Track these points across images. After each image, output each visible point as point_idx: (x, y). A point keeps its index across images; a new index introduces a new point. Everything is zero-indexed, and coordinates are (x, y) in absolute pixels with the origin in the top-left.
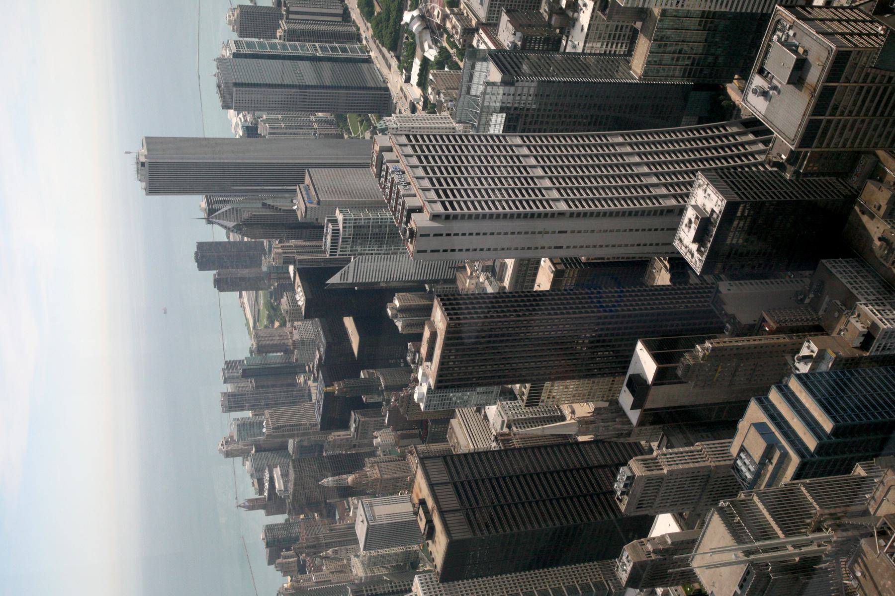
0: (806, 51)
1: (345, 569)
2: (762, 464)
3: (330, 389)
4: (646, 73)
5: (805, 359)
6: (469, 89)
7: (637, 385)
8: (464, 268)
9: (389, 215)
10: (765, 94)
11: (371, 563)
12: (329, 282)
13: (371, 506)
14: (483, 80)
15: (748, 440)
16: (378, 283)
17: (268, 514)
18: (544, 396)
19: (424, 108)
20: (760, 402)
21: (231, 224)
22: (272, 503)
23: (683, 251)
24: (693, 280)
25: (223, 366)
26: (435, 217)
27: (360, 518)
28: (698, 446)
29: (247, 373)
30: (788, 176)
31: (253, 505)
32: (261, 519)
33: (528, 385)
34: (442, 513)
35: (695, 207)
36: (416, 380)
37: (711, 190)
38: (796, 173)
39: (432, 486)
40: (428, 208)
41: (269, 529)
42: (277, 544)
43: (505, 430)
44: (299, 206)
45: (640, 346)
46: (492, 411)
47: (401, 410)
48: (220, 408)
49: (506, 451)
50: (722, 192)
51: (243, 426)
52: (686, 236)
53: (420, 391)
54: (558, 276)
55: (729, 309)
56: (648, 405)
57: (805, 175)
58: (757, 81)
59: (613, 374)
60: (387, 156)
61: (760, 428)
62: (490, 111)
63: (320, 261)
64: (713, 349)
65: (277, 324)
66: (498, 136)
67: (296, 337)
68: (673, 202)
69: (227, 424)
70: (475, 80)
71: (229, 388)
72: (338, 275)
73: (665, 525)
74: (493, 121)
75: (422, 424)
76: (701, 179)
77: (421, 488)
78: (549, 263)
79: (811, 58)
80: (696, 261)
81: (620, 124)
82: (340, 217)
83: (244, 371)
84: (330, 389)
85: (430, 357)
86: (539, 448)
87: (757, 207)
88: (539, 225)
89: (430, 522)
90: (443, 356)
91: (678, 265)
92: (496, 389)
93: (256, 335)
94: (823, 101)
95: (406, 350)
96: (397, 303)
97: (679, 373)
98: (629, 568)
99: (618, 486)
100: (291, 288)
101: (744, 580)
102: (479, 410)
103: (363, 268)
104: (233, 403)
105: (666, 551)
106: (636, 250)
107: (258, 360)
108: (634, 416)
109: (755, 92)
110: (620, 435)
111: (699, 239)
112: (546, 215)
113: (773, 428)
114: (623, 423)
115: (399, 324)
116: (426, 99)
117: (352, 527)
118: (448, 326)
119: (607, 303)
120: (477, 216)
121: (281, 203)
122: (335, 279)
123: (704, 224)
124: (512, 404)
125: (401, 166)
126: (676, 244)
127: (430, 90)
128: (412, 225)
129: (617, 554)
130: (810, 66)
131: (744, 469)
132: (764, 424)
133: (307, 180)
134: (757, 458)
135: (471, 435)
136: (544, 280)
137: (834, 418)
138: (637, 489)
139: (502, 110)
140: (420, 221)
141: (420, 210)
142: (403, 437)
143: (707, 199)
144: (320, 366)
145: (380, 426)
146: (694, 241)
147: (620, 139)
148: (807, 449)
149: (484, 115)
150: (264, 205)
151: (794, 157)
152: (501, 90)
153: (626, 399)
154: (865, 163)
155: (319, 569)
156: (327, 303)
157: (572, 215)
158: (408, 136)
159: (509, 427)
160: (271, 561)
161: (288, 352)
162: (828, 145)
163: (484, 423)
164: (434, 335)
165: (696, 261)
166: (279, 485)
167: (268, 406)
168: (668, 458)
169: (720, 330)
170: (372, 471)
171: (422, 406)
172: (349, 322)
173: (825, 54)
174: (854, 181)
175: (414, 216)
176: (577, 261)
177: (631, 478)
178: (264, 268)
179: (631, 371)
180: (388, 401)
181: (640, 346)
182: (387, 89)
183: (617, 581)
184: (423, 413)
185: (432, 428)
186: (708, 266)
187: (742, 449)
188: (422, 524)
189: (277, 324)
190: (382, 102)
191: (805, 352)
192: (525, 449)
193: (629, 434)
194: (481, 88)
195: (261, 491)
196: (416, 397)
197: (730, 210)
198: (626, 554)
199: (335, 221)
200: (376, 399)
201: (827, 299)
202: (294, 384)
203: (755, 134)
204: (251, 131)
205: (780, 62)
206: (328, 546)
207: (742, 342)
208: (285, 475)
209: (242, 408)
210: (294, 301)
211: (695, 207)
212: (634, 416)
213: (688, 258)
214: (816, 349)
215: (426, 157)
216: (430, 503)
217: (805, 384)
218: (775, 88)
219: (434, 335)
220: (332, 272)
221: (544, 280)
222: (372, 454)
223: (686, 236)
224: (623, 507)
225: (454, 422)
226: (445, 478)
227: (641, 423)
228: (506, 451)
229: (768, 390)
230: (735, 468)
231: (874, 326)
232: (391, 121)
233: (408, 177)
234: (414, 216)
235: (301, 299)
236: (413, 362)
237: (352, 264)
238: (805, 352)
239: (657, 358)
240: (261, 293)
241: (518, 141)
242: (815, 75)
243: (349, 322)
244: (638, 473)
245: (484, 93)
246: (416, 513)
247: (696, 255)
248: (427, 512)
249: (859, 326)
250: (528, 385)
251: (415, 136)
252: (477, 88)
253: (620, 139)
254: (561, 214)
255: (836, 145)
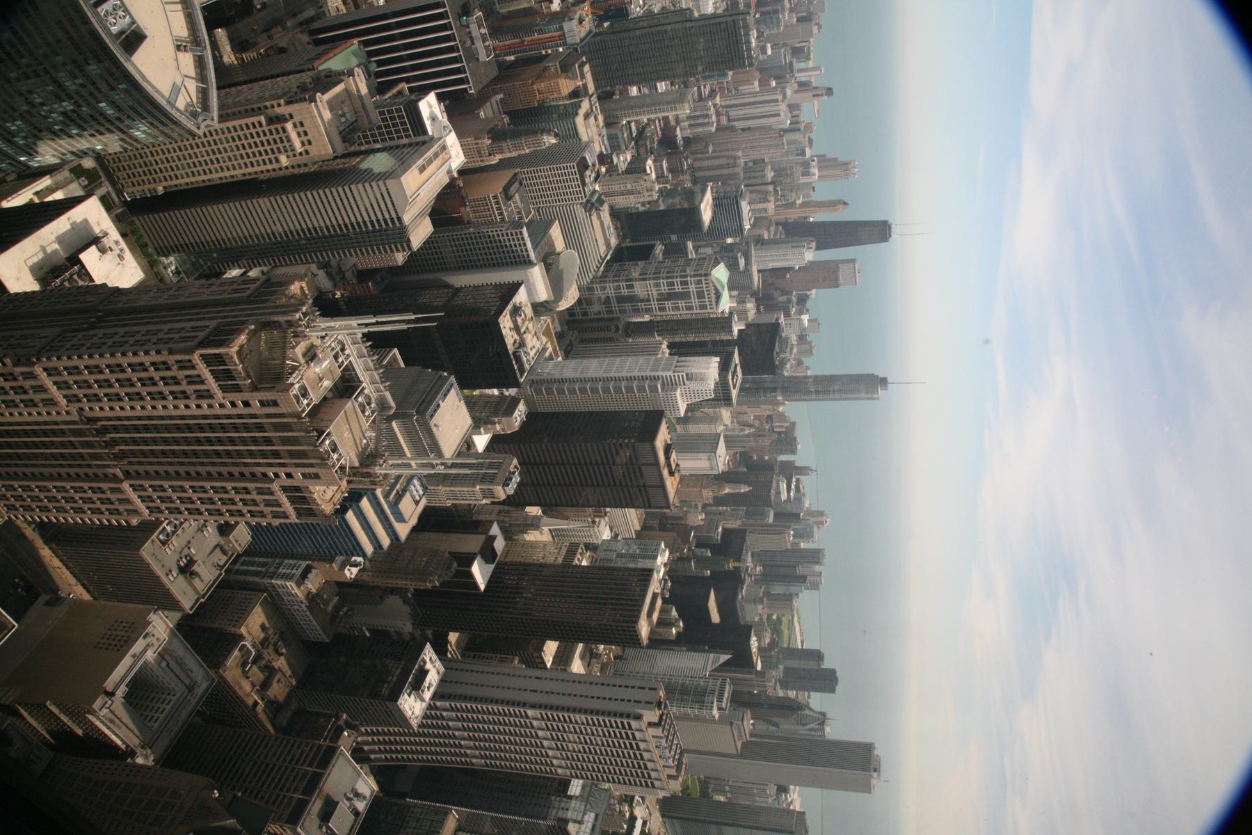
0: (320, 827)
1: (735, 415)
2: (404, 490)
3: (737, 564)
4: (446, 813)
5: (355, 565)
6: (597, 816)
7: (488, 554)
8: (615, 658)
9: (674, 710)
10: (357, 795)
11: (715, 419)
12: (729, 656)
13: (711, 468)
14: (583, 827)
15: (411, 509)
16: (688, 650)
17: (792, 463)
18: (564, 551)
19: (633, 797)
20: (397, 539)
21: (807, 712)
22: (790, 471)
23: (438, 663)
24: (429, 633)
25: (821, 587)
26: (638, 717)
27: (723, 458)
28: (449, 503)
29: (803, 579)
30: (345, 716)
31: (803, 470)
32: (799, 459)
33: (576, 562)
34: (657, 464)
35: (423, 700)
36: (665, 565)
37: (408, 713)
38: (338, 718)
39: (662, 486)
40: (643, 725)
41: (793, 451)
42: (787, 440)
43: (597, 520)
44: (749, 723)
45: (482, 587)
46: (606, 535)
47: (679, 541)
48: (826, 553)
49: (599, 507)
50: (399, 710)
51: (808, 536)
52: (433, 678)
53: (663, 558)
54: (540, 649)
55: (406, 609)
56: (483, 537)
57: (331, 716)
58: (361, 806)
59: (505, 563)
60: (673, 772)
61: (400, 518)
62: (580, 797)
63: (735, 672)
64: (425, 581)
65: (774, 617)
66: (577, 777)
67: (760, 607)
68: (438, 704)
69: (820, 539)
70: (590, 825)
71: (817, 568)
72: (721, 661)
73: (481, 441)
74: (579, 789)
75: (663, 528)
76: (414, 723)
77: (671, 484)
78: (546, 659)
79: (317, 822)
80: (428, 653)
81: (471, 773)
82: (715, 713)
83: (804, 581)
84: (737, 564)
85: (655, 596)
86: (573, 506)
87: (374, 694)
88: (554, 700)
89: (668, 458)
90: (644, 596)
91: (441, 650)
92: (601, 554)
93: (792, 610)
94: (314, 782)
95: (671, 591)
96: (674, 630)
97: (455, 564)
98: (517, 413)
99: (516, 479)
100: (759, 649)
101: (435, 411)
102: (616, 535)
103: (698, 664)
104: (815, 556)
105: (486, 423)
106: (476, 668)
107: (793, 589)
108: (495, 530)
109: (365, 798)
110: (508, 512)
111: (423, 673)
112: (546, 707)
113: (391, 518)
114: (503, 522)
115: (674, 613)
116: (631, 806)
117: (727, 448)
118: (636, 622)
119: (503, 621)
120: (603, 713)
121: (762, 727)
122: (724, 658)
123: (417, 686)
124: (588, 540)
125: (662, 762)
126: (442, 669)
127: (627, 815)
128: (658, 713)
129: (524, 425)
130: (318, 815)
131: (419, 487)
132: (398, 521)
133: (739, 744)
134: (408, 494)
135: (626, 519)
136: (551, 647)
137: (345, 521)
138: (501, 477)
139: (570, 797)
140: (651, 715)
141: (650, 724)
142: (680, 518)
143: (412, 706)
144: (743, 583)
145: (697, 528)
146: (427, 671)
147: (474, 760)
148: (369, 500)
149: (586, 795)
150: (777, 726)
151: (337, 734)
152: (569, 815)
153: (499, 544)
154: (283, 720)
155: (757, 417)
156: (730, 638)
157: (524, 705)
158: (653, 786)
159: (594, 522)
160: (794, 424)
161: (767, 594)
162: (314, 745)
163: (614, 527)
164: (650, 615)
165: (428, 653)
166: (783, 486)
167: (787, 551)
168: (473, 496)
169: (417, 592)
170: (708, 494)
171: (663, 545)
172: (715, 618)
173: (306, 824)
174: (294, 706)
175: (656, 720)
176: (521, 661)
177: (506, 484)
178: (781, 667)
179: (492, 567)
180: (690, 549)
181: (482, 587)
182: (663, 816)
183: (527, 404)
184: (662, 538)
185: (655, 523)
186: (421, 649)
187: (417, 503)
188: (674, 456)
189: (774, 617)
190: (668, 807)
191: (355, 570)
192: (583, 506)
193: (500, 512)
194: (586, 817)
195: (798, 481)
196: (667, 553)
197: (395, 696)
198: (517, 424)
199: (720, 709)
200: (699, 551)
201: (330, 608)
202: (763, 566)
203: (362, 750)
204: (783, 789)
205: (342, 821)
206: (748, 435)
207: (402, 583)
208: (778, 493)
209: (806, 550)
210: (759, 640)
211: (423, 700)
212: (495, 530)
213: (435, 657)
214: (346, 572)
215: (640, 767)
216: (665, 472)
217: (361, 549)
218: (349, 799)
219: (650, 615)
220: (726, 664)
221: (551, 647)
222: (705, 506)
223: (433, 678)
224: (515, 461)
225: (638, 528)
226: (651, 491)
227: (491, 523)
228: (600, 506)
229: (390, 546)
230: (425, 488)
231: (299, 584)
232: (661, 794)
233: (657, 752)
234: (656, 720)
235: (754, 643)
236: (666, 581)
237: (709, 669)
238: (355, 570)
239: (471, 576)
240: (785, 645)
241: (560, 771)
242: (316, 806)
243: (715, 618)
244: (500, 488)
245: (584, 814)
246: (677, 465)
247: (427, 659)
248: (669, 466)
249: (310, 586)
250: (576, 562)
251: (647, 785)
252: (590, 817)
253: (474, 760)
254: (533, 706)
255: (307, 745)
